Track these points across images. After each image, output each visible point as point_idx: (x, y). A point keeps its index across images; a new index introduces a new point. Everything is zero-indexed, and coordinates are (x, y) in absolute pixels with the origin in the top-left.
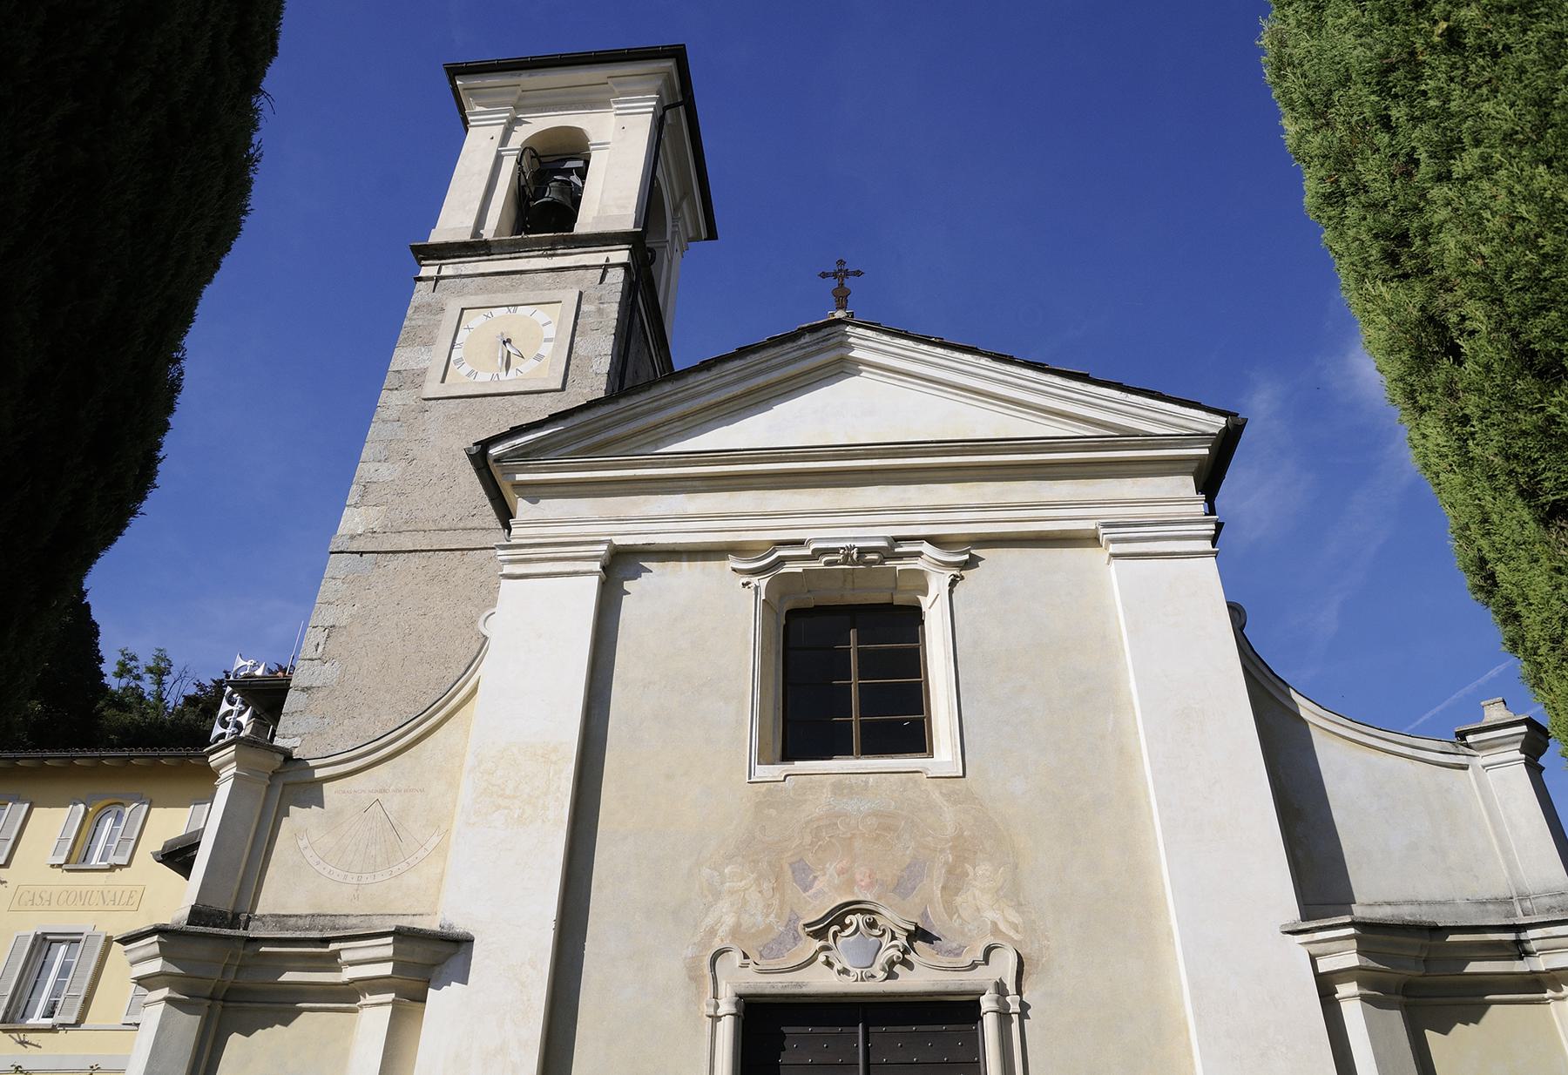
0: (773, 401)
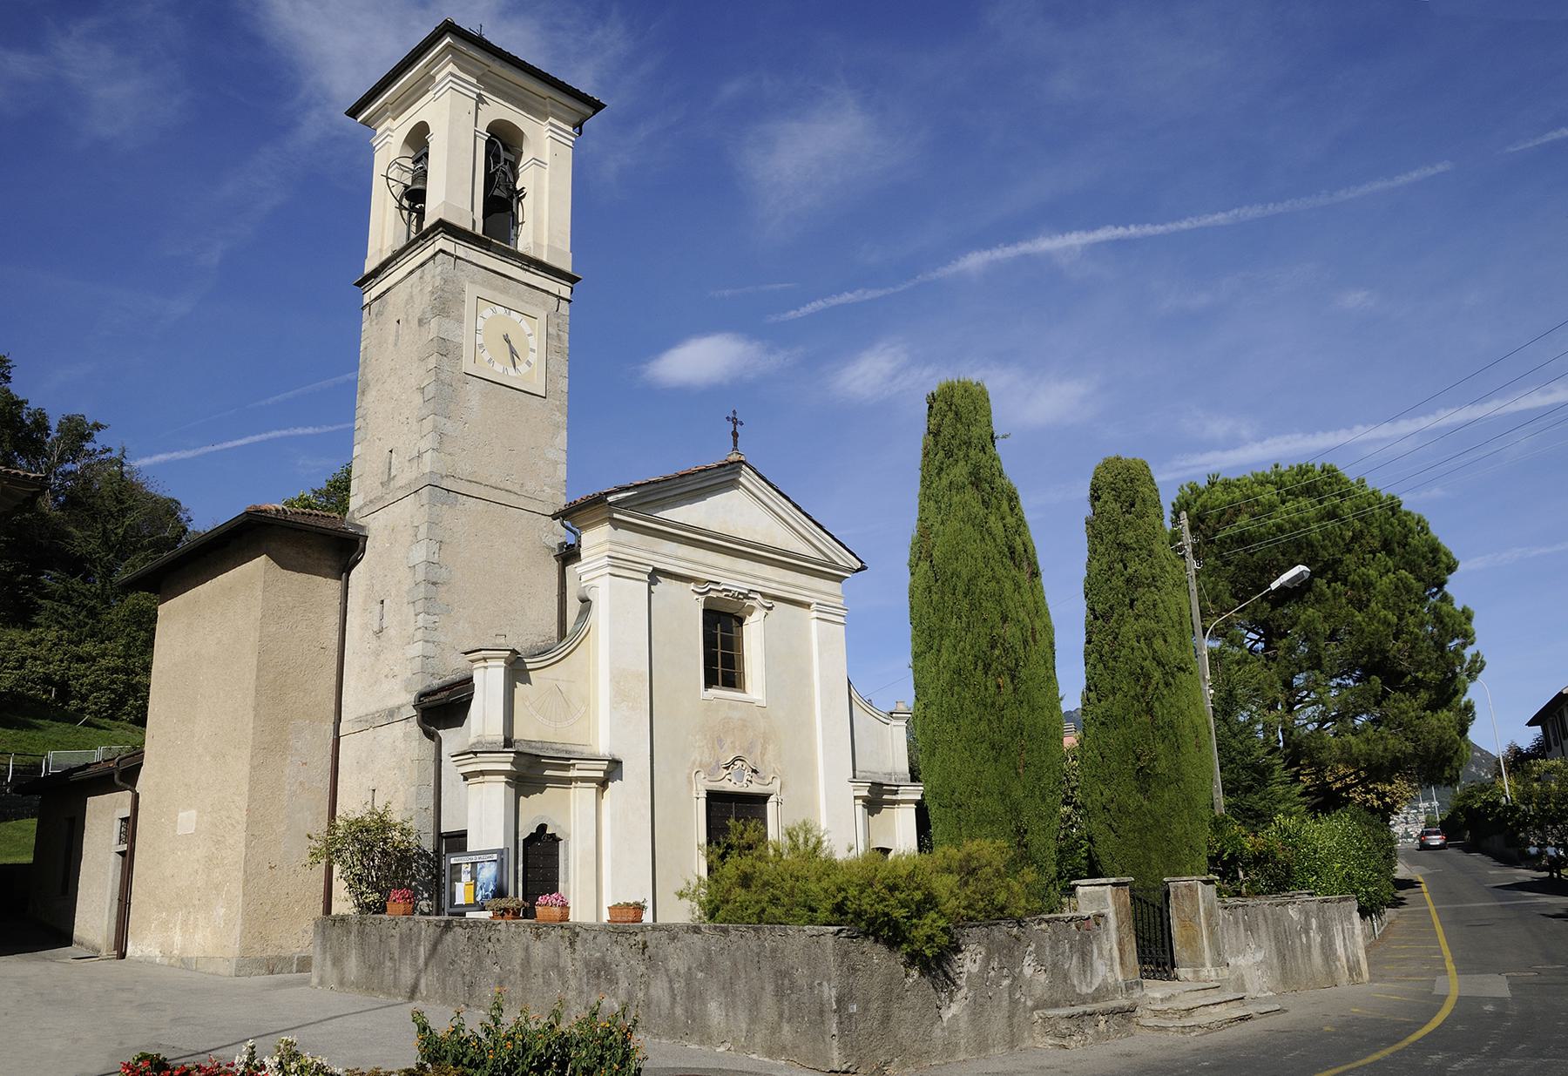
0: (707, 495)
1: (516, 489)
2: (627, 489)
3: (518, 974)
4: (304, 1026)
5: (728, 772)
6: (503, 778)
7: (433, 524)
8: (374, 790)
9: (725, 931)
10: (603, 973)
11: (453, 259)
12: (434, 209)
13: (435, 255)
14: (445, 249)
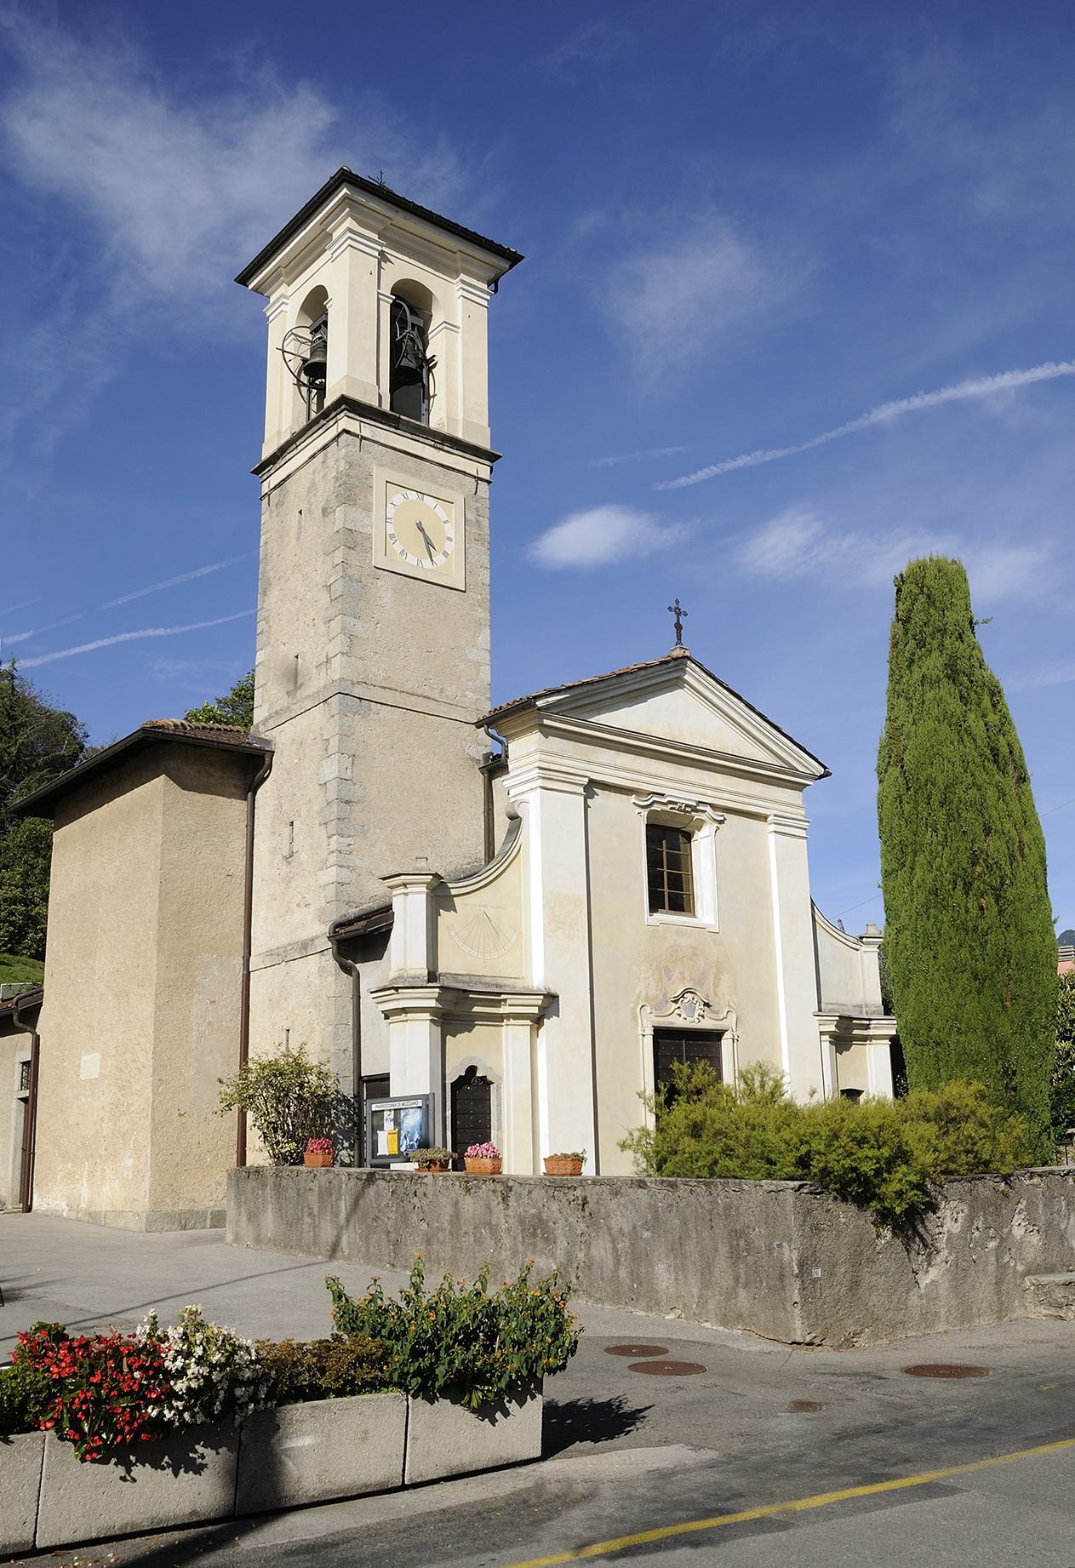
0: (648, 696)
1: (435, 695)
2: (558, 692)
3: (447, 1231)
4: (217, 1286)
5: (677, 1006)
6: (427, 1016)
7: (344, 736)
8: (288, 1030)
9: (673, 1186)
10: (539, 1231)
11: (358, 440)
12: (336, 384)
13: (338, 436)
14: (348, 429)
